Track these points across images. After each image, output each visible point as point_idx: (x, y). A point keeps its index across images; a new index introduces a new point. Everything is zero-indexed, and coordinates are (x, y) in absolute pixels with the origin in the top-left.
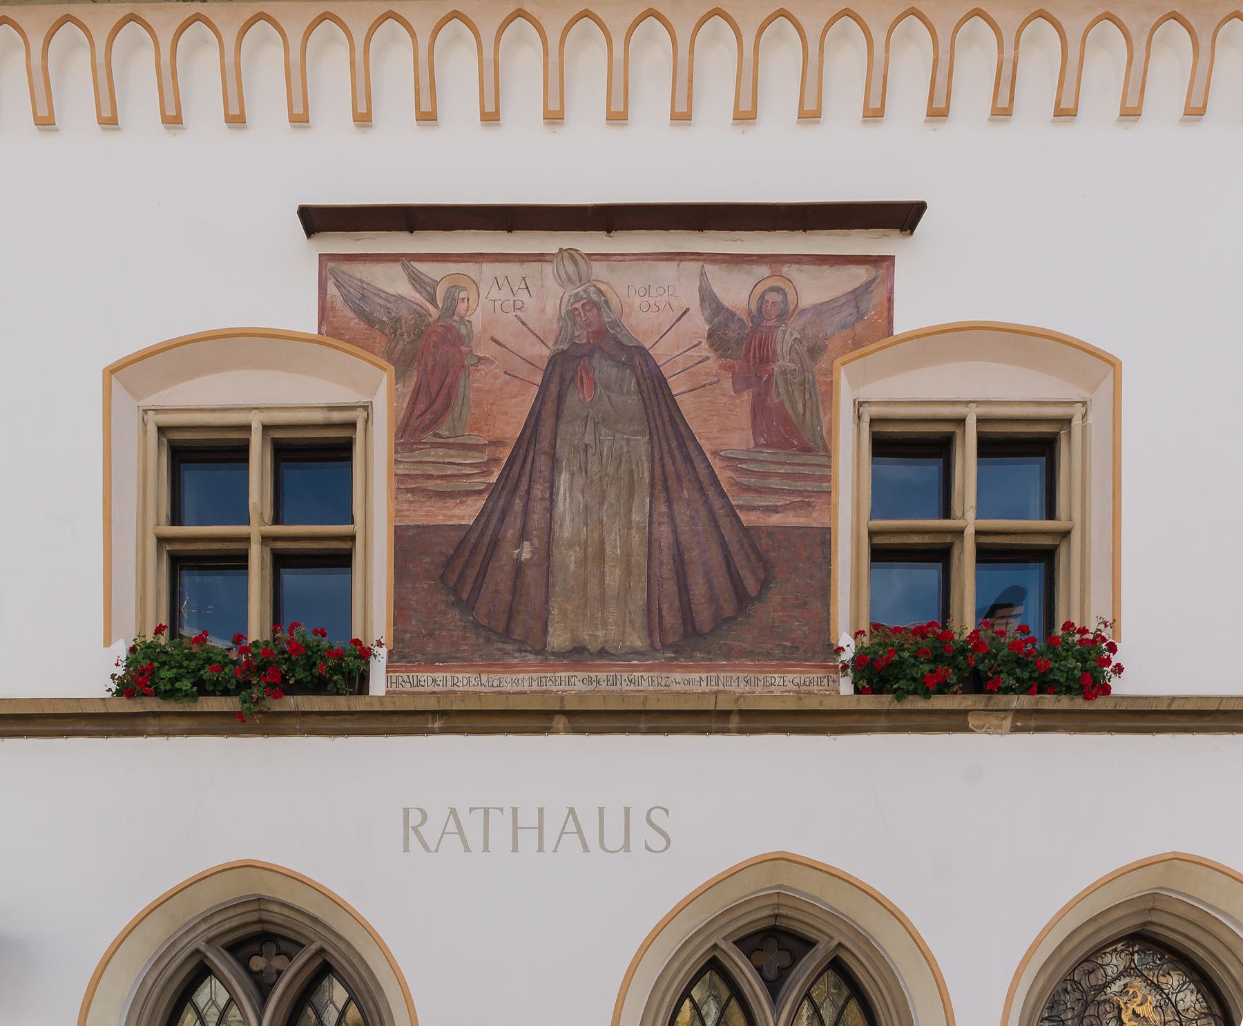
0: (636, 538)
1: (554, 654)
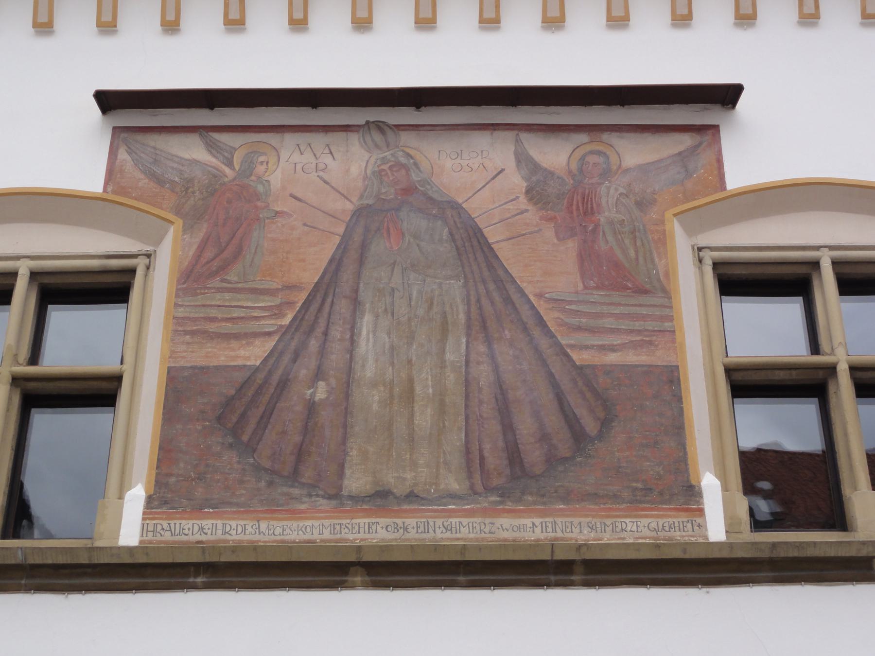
0: (451, 378)
1: (351, 497)
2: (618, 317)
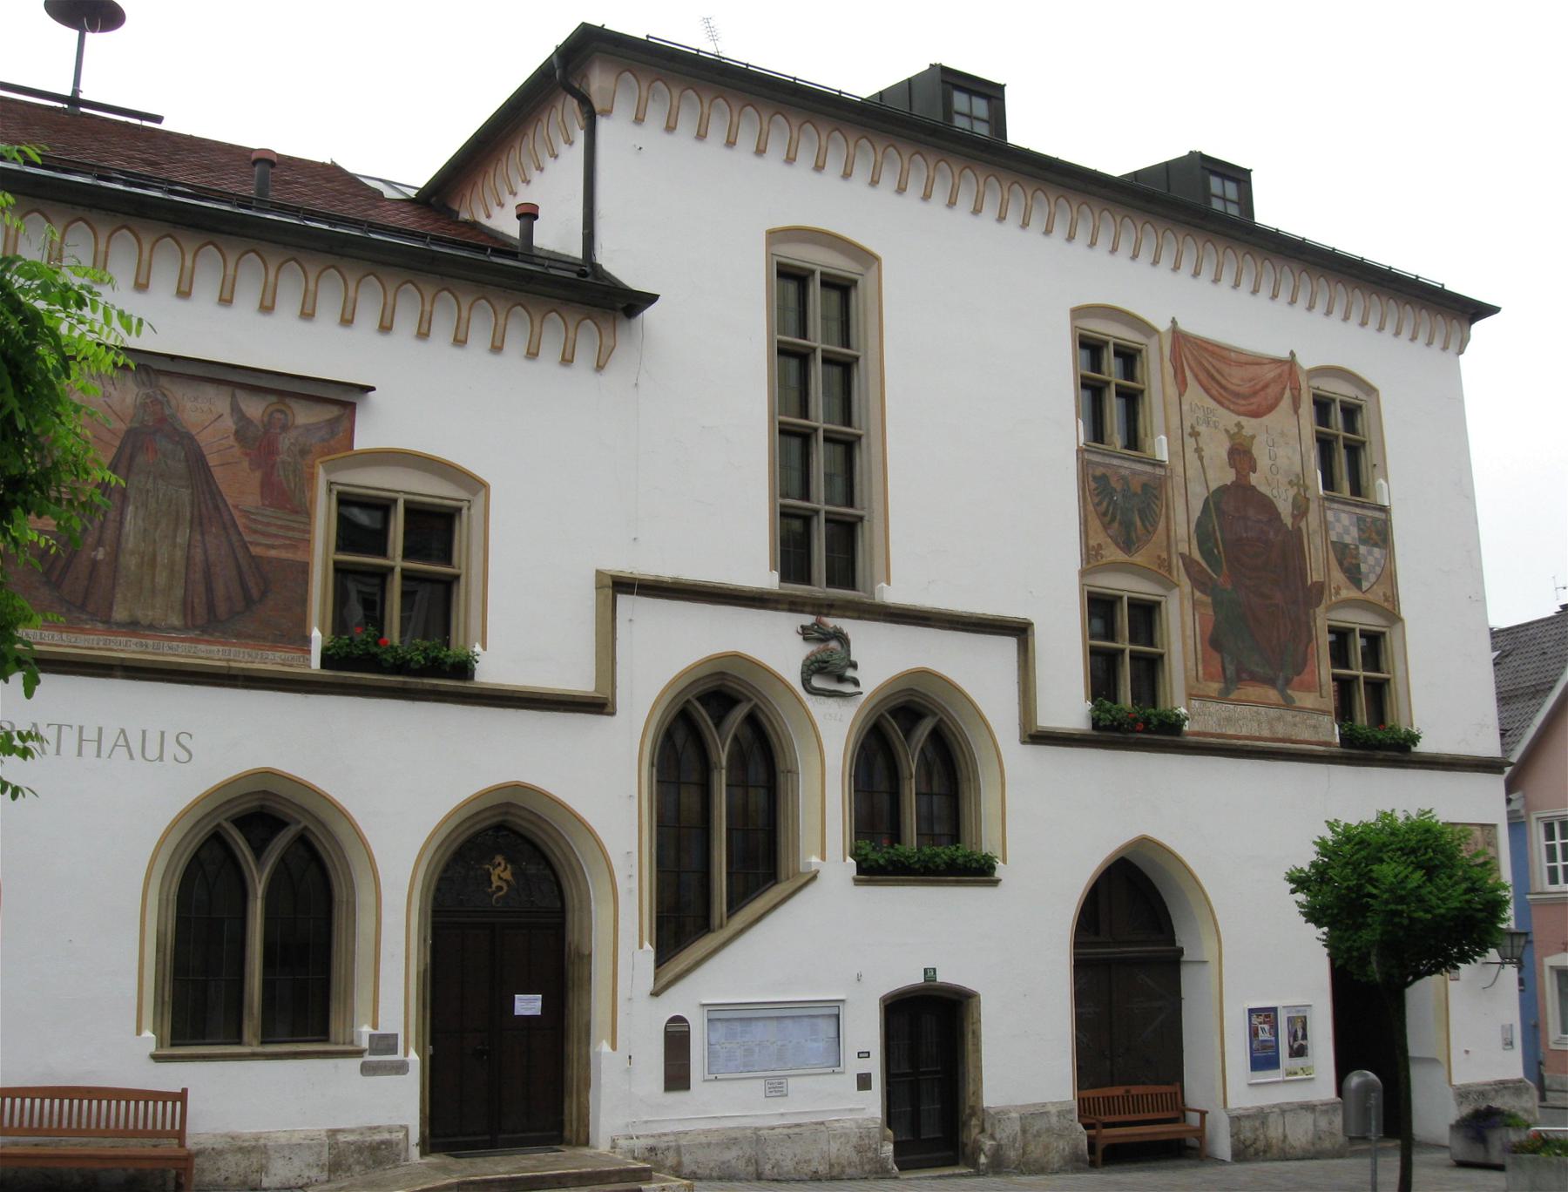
0: (179, 554)
2: (281, 527)
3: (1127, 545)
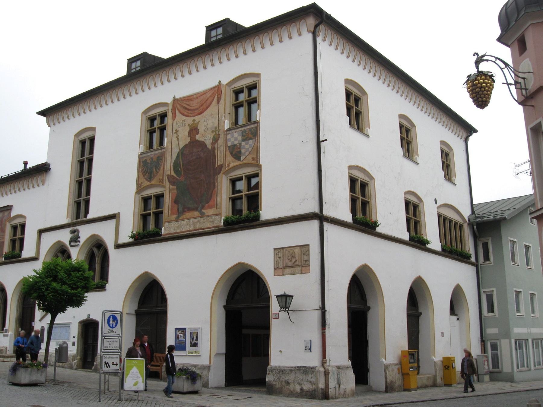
3: (150, 179)
